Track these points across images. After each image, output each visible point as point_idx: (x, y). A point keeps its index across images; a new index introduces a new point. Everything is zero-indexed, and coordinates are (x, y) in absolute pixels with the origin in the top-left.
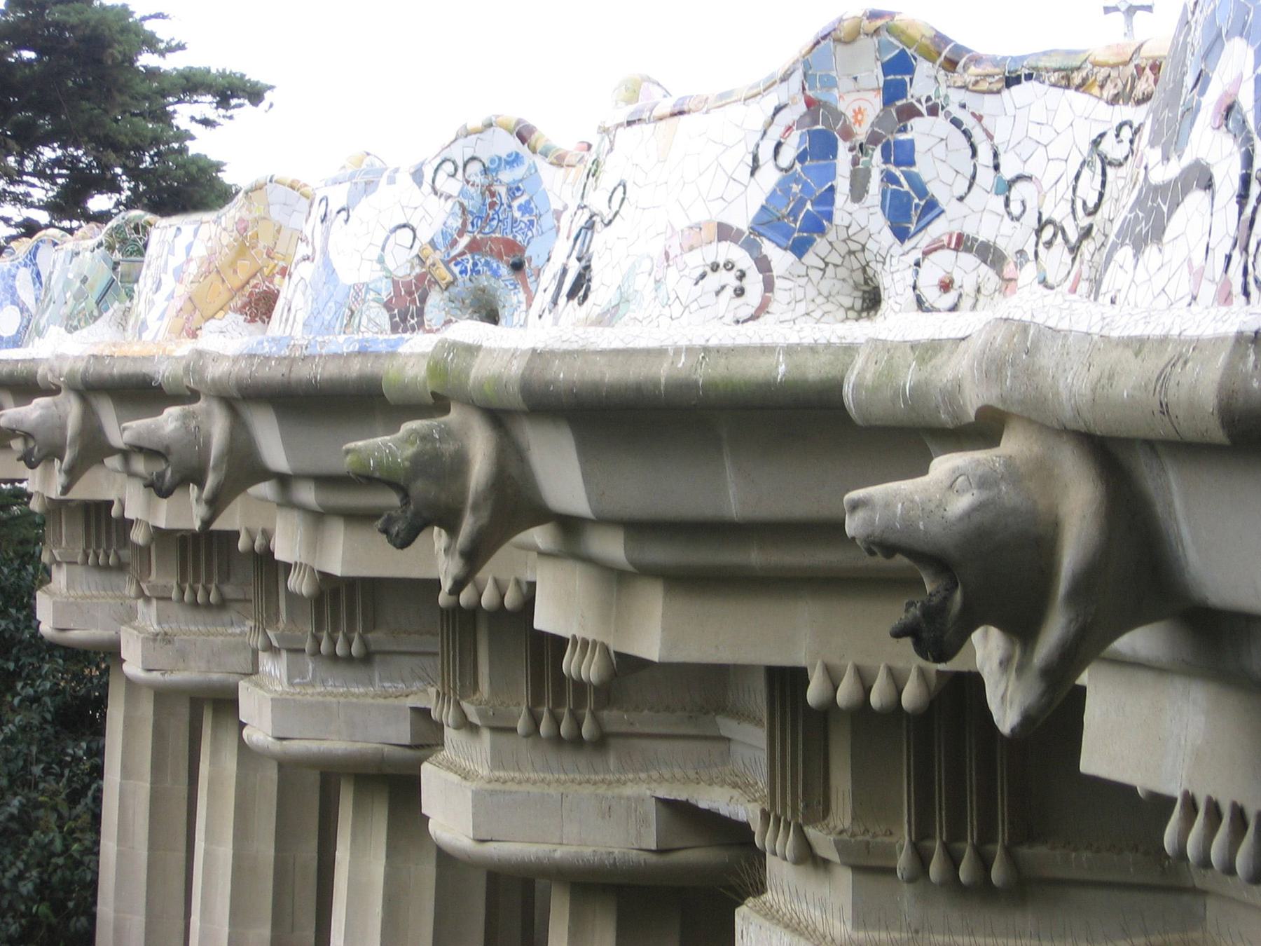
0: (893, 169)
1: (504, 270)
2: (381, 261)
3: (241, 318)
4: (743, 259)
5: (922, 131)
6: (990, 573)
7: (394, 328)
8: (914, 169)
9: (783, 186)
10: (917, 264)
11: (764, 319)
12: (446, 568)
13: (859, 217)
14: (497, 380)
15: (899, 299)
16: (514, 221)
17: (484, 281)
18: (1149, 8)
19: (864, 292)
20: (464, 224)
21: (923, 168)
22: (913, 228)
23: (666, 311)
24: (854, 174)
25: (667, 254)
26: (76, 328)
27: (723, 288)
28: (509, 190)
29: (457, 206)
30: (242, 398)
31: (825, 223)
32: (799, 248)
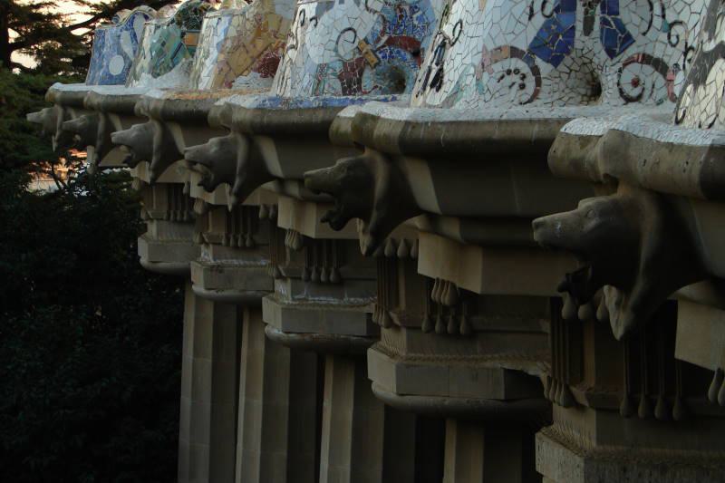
0: (607, 17)
1: (408, 56)
2: (336, 50)
3: (259, 75)
6: (604, 256)
8: (619, 17)
9: (546, 27)
10: (620, 71)
11: (536, 102)
12: (365, 242)
15: (610, 91)
16: (414, 26)
19: (593, 85)
20: (384, 28)
22: (618, 50)
23: (482, 97)
24: (585, 19)
25: (483, 64)
26: (159, 75)
27: (514, 84)
28: (411, 7)
29: (380, 18)
31: (570, 47)
32: (555, 61)
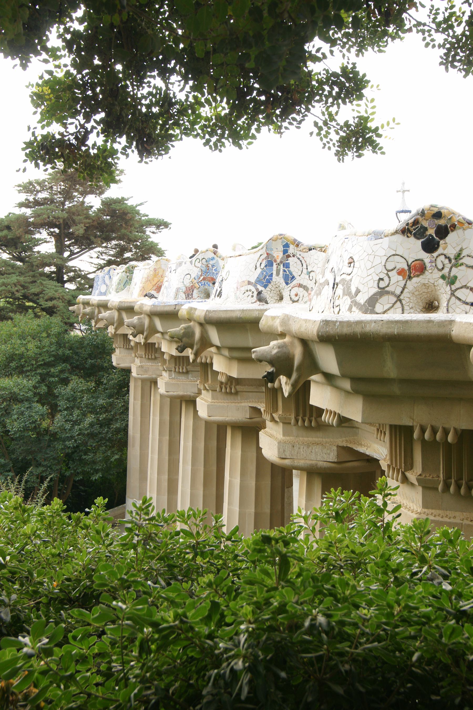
1: (211, 285)
4: (253, 289)
5: (291, 260)
7: (186, 298)
12: (192, 357)
13: (278, 280)
14: (200, 316)
17: (206, 287)
18: (409, 191)
21: (292, 269)
24: (277, 270)
30: (152, 314)
32: (265, 286)
